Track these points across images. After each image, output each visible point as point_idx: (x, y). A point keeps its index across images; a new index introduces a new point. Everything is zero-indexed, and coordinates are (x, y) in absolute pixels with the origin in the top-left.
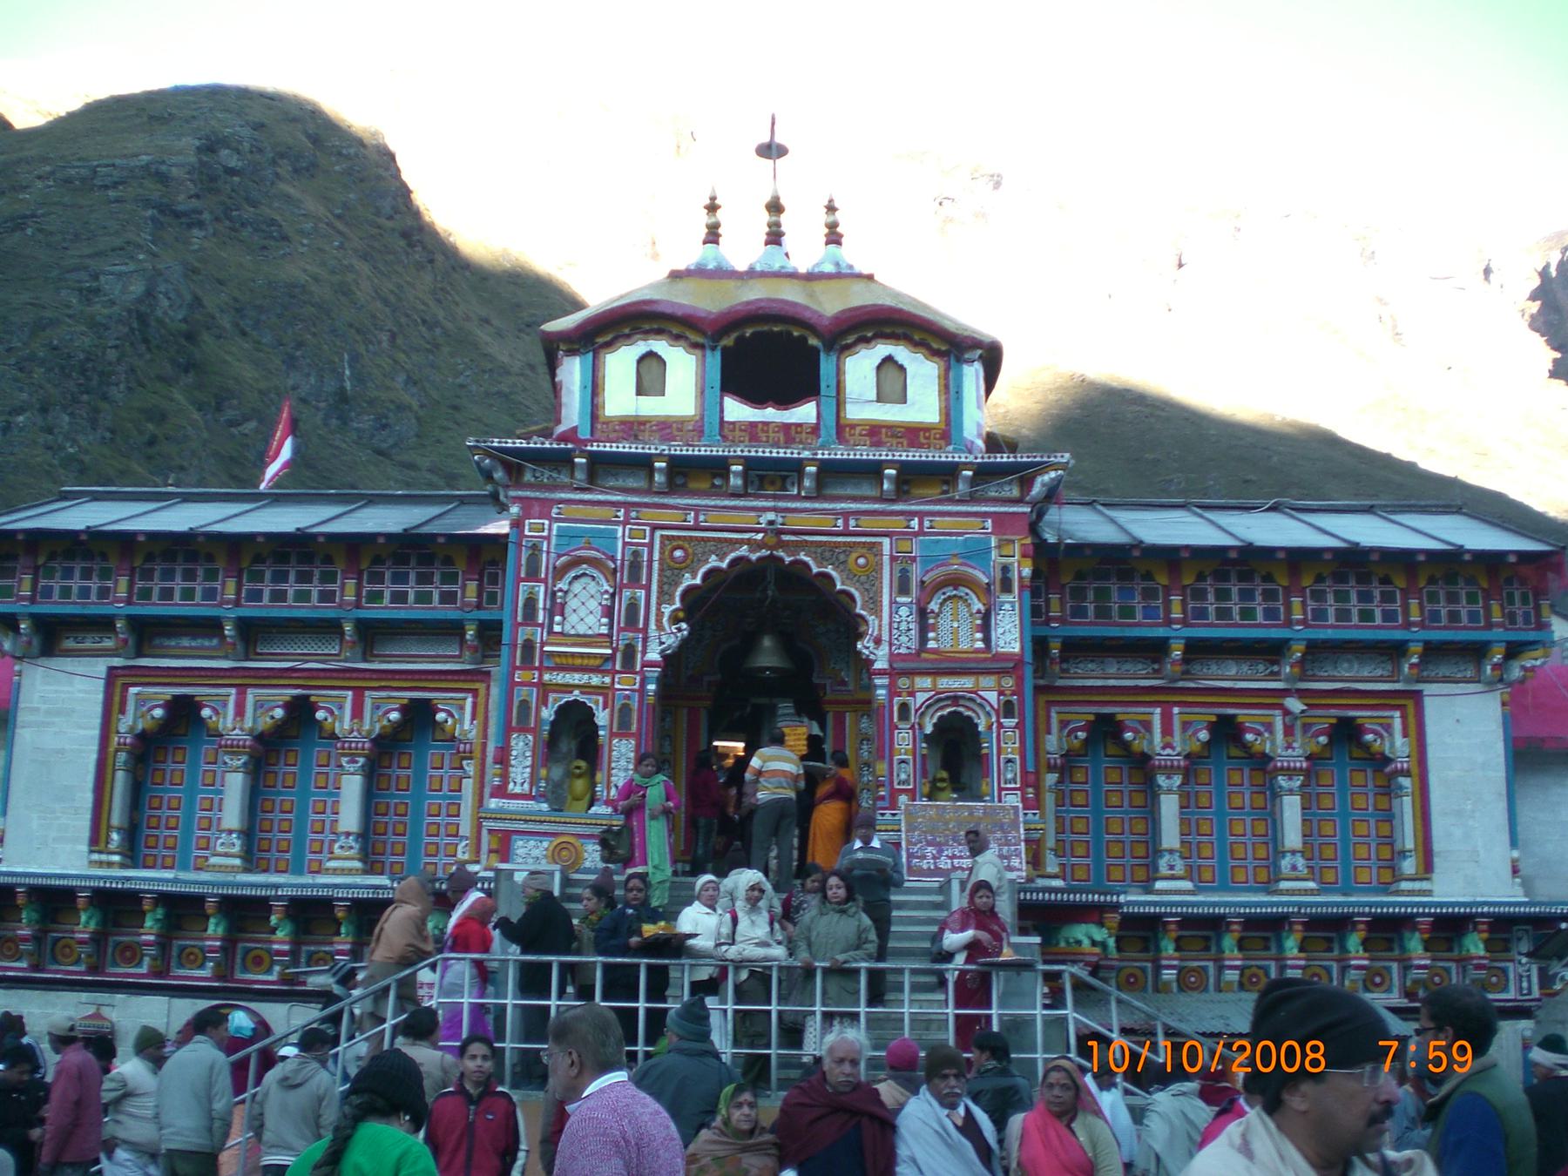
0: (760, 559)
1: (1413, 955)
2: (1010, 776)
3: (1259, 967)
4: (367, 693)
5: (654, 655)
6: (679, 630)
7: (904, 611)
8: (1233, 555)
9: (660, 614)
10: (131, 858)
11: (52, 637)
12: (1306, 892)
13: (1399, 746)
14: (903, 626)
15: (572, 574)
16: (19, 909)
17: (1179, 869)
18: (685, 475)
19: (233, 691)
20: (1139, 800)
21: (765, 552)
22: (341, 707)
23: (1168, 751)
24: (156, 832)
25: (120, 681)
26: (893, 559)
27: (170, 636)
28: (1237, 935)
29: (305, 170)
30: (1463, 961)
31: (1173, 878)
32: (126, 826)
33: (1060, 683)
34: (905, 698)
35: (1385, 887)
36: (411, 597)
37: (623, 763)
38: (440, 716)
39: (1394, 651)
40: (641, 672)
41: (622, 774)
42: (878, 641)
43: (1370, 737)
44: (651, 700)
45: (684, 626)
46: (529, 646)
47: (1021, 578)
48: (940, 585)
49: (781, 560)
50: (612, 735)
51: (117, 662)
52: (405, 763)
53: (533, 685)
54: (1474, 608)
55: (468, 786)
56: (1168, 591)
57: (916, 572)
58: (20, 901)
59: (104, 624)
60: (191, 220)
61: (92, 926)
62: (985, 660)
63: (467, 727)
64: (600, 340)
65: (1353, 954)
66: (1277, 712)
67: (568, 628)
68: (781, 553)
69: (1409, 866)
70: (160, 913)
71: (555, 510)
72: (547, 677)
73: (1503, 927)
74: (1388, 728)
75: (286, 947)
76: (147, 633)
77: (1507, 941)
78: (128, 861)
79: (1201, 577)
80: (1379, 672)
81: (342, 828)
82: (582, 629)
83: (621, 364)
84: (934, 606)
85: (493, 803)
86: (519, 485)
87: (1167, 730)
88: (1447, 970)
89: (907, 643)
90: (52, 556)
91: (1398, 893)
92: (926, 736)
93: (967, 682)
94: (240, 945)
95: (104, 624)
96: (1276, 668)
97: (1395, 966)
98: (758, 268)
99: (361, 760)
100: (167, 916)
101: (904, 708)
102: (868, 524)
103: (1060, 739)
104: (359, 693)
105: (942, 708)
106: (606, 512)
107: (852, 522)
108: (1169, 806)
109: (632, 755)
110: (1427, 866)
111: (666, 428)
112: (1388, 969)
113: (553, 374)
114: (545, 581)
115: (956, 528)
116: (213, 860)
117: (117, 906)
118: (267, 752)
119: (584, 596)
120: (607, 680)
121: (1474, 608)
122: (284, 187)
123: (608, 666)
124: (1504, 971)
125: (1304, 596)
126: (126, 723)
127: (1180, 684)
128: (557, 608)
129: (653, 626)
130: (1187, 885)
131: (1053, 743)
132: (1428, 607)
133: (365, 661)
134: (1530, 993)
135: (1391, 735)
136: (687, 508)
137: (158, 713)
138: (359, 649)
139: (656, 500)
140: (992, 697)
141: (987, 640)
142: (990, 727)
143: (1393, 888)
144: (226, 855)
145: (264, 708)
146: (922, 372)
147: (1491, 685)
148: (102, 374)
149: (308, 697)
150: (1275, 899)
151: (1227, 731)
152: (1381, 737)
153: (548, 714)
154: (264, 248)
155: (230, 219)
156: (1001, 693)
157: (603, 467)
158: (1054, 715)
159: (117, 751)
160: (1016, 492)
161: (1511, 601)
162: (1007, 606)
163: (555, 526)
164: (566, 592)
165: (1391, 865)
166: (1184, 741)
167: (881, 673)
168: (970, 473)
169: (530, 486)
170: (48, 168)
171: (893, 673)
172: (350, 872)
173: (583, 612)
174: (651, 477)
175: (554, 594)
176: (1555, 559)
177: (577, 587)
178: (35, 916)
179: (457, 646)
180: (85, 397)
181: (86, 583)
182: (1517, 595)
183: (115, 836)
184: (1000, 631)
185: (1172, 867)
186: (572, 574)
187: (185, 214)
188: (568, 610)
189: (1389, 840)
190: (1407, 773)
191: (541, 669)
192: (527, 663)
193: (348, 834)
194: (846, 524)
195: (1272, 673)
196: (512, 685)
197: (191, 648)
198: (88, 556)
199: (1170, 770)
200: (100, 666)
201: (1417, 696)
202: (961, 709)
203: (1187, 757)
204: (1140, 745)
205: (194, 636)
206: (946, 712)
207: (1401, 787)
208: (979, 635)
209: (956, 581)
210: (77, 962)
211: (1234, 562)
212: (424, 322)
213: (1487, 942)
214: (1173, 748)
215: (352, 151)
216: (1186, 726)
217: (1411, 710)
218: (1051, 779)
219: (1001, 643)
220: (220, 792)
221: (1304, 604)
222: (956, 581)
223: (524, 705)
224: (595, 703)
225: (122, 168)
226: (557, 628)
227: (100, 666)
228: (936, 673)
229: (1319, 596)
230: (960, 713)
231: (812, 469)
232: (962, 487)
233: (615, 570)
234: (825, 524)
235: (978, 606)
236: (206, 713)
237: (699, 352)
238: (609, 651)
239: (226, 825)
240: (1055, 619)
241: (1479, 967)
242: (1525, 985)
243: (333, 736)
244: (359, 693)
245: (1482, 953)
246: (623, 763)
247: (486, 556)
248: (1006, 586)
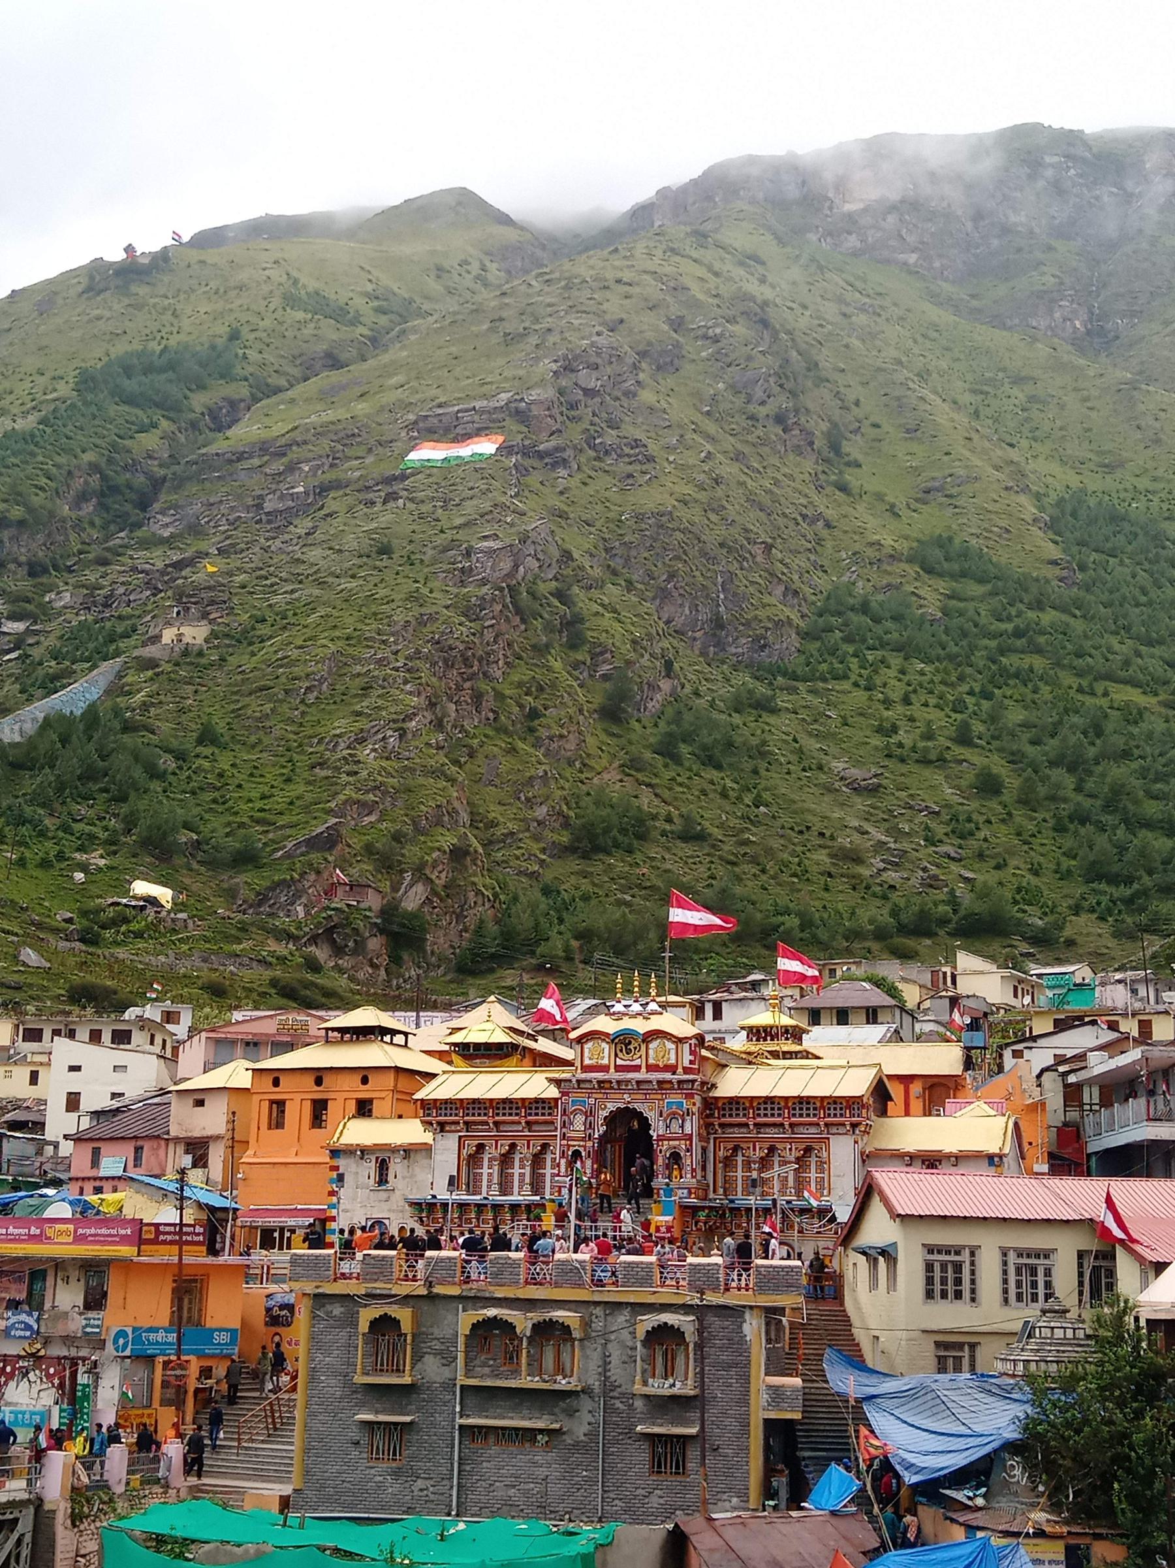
11: (442, 1126)
29: (666, 361)
59: (458, 1123)
60: (555, 460)
115: (675, 1098)
122: (647, 396)
131: (721, 1154)
146: (670, 1046)
148: (480, 660)
154: (630, 476)
155: (593, 447)
170: (412, 417)
180: (467, 685)
187: (548, 453)
212: (804, 517)
215: (718, 331)
225: (482, 412)
228: (669, 1139)
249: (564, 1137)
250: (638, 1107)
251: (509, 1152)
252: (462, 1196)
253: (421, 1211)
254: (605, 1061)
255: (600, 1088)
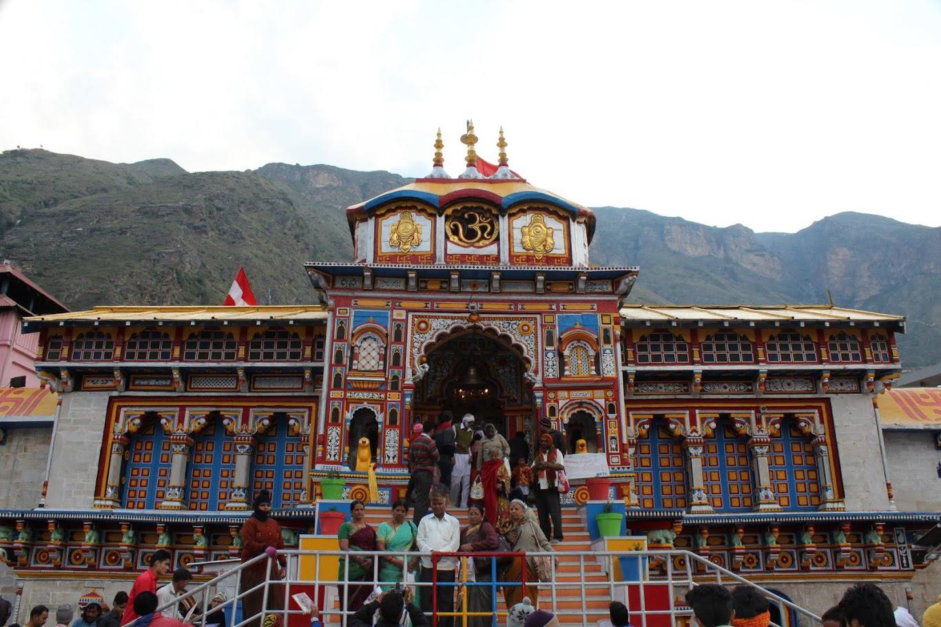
0: (469, 328)
1: (841, 544)
2: (614, 446)
3: (753, 553)
4: (251, 409)
5: (409, 380)
6: (424, 367)
7: (550, 355)
8: (726, 324)
9: (412, 359)
10: (120, 503)
11: (79, 380)
12: (775, 510)
13: (819, 429)
14: (550, 363)
15: (364, 336)
16: (49, 533)
17: (704, 501)
18: (426, 282)
19: (178, 409)
20: (678, 462)
21: (471, 324)
22: (236, 417)
23: (694, 434)
24: (134, 488)
25: (116, 405)
26: (542, 326)
27: (143, 379)
28: (742, 535)
30: (869, 549)
31: (701, 504)
32: (117, 483)
33: (635, 398)
34: (553, 403)
35: (816, 508)
36: (275, 356)
37: (392, 443)
38: (292, 422)
39: (817, 375)
40: (402, 392)
41: (392, 449)
42: (536, 372)
43: (803, 424)
44: (408, 407)
45: (426, 365)
46: (338, 376)
47: (615, 336)
48: (571, 339)
49: (480, 328)
50: (386, 427)
51: (115, 394)
52: (272, 448)
53: (340, 399)
54: (855, 352)
55: (307, 460)
56: (691, 345)
57: (557, 332)
58: (51, 528)
61: (92, 542)
62: (597, 381)
63: (307, 429)
64: (378, 213)
65: (807, 545)
66: (753, 412)
67: (360, 367)
68: (479, 324)
69: (829, 495)
70: (131, 533)
71: (353, 302)
72: (348, 395)
73: (892, 526)
74: (812, 419)
75: (202, 552)
76: (130, 375)
77: (891, 536)
78: (118, 505)
79: (708, 338)
80: (806, 388)
81: (236, 484)
82: (368, 367)
83: (389, 224)
84: (566, 353)
85: (318, 467)
86: (333, 288)
87: (693, 422)
88: (859, 553)
89: (552, 373)
90: (81, 336)
91: (825, 509)
92: (565, 425)
93: (588, 394)
94: (177, 552)
95: (108, 373)
96: (750, 387)
97: (828, 551)
98: (464, 177)
99: (248, 446)
100: (134, 535)
101: (552, 409)
102: (528, 307)
103: (635, 430)
104: (246, 409)
105: (574, 409)
106: (383, 303)
107: (520, 307)
108: (696, 464)
109: (397, 438)
110: (841, 494)
111: (415, 258)
112: (825, 553)
113: (353, 234)
114: (346, 341)
116: (165, 503)
117: (106, 528)
118: (196, 442)
119: (369, 349)
120: (383, 396)
121: (855, 352)
123: (383, 388)
124: (892, 553)
125: (764, 347)
126: (119, 427)
127: (698, 397)
128: (353, 356)
129: (408, 365)
130: (710, 508)
132: (831, 352)
133: (250, 391)
134: (908, 566)
135: (814, 422)
136: (427, 300)
137: (137, 421)
138: (246, 384)
139: (410, 296)
140: (602, 402)
141: (598, 370)
142: (601, 419)
143: (821, 507)
144: (171, 500)
145: (194, 419)
147: (866, 394)
149: (219, 412)
150: (758, 514)
151: (725, 423)
152: (809, 424)
153: (349, 416)
156: (606, 400)
157: (377, 274)
158: (631, 415)
159: (113, 443)
160: (610, 289)
161: (876, 349)
162: (608, 351)
163: (353, 311)
164: (359, 347)
165: (819, 493)
166: (702, 429)
167: (538, 389)
168: (585, 278)
169: (339, 289)
171: (545, 389)
172: (240, 509)
173: (369, 358)
174: (407, 283)
175: (352, 348)
176: (901, 325)
177: (365, 344)
178: (58, 536)
179: (300, 383)
181: (98, 350)
182: (878, 344)
183: (109, 490)
184: (604, 365)
185: (700, 499)
186: (364, 336)
188: (360, 358)
189: (816, 481)
190: (825, 443)
191: (345, 391)
192: (337, 387)
193: (239, 488)
194: (516, 307)
195: (748, 390)
196: (328, 399)
197: (155, 385)
198: (101, 335)
199: (695, 444)
200: (105, 397)
201: (827, 401)
202: (585, 410)
203: (706, 437)
204: (679, 431)
205: (157, 379)
206: (575, 411)
207: (822, 451)
208: (594, 368)
209: (579, 338)
210: (83, 563)
211: (726, 329)
213: (882, 536)
214: (697, 432)
216: (703, 420)
217: (824, 409)
218: (631, 451)
219: (606, 372)
220: (170, 466)
221: (764, 352)
222: (579, 338)
223: (336, 410)
224: (376, 409)
226: (354, 367)
227: (105, 397)
228: (569, 389)
229: (772, 347)
230: (584, 412)
231: (497, 277)
232: (581, 286)
233: (387, 335)
234: (505, 307)
235: (592, 353)
236: (163, 421)
237: (433, 219)
238: (384, 379)
239: (171, 484)
240: (631, 362)
241: (881, 551)
242: (905, 561)
243: (232, 434)
244: (246, 409)
245: (880, 543)
246: (392, 443)
247: (314, 329)
248: (607, 341)
249: (337, 383)
250: (499, 326)
251: (204, 429)
252: (106, 507)
253: (16, 534)
254: (425, 247)
255: (420, 290)
